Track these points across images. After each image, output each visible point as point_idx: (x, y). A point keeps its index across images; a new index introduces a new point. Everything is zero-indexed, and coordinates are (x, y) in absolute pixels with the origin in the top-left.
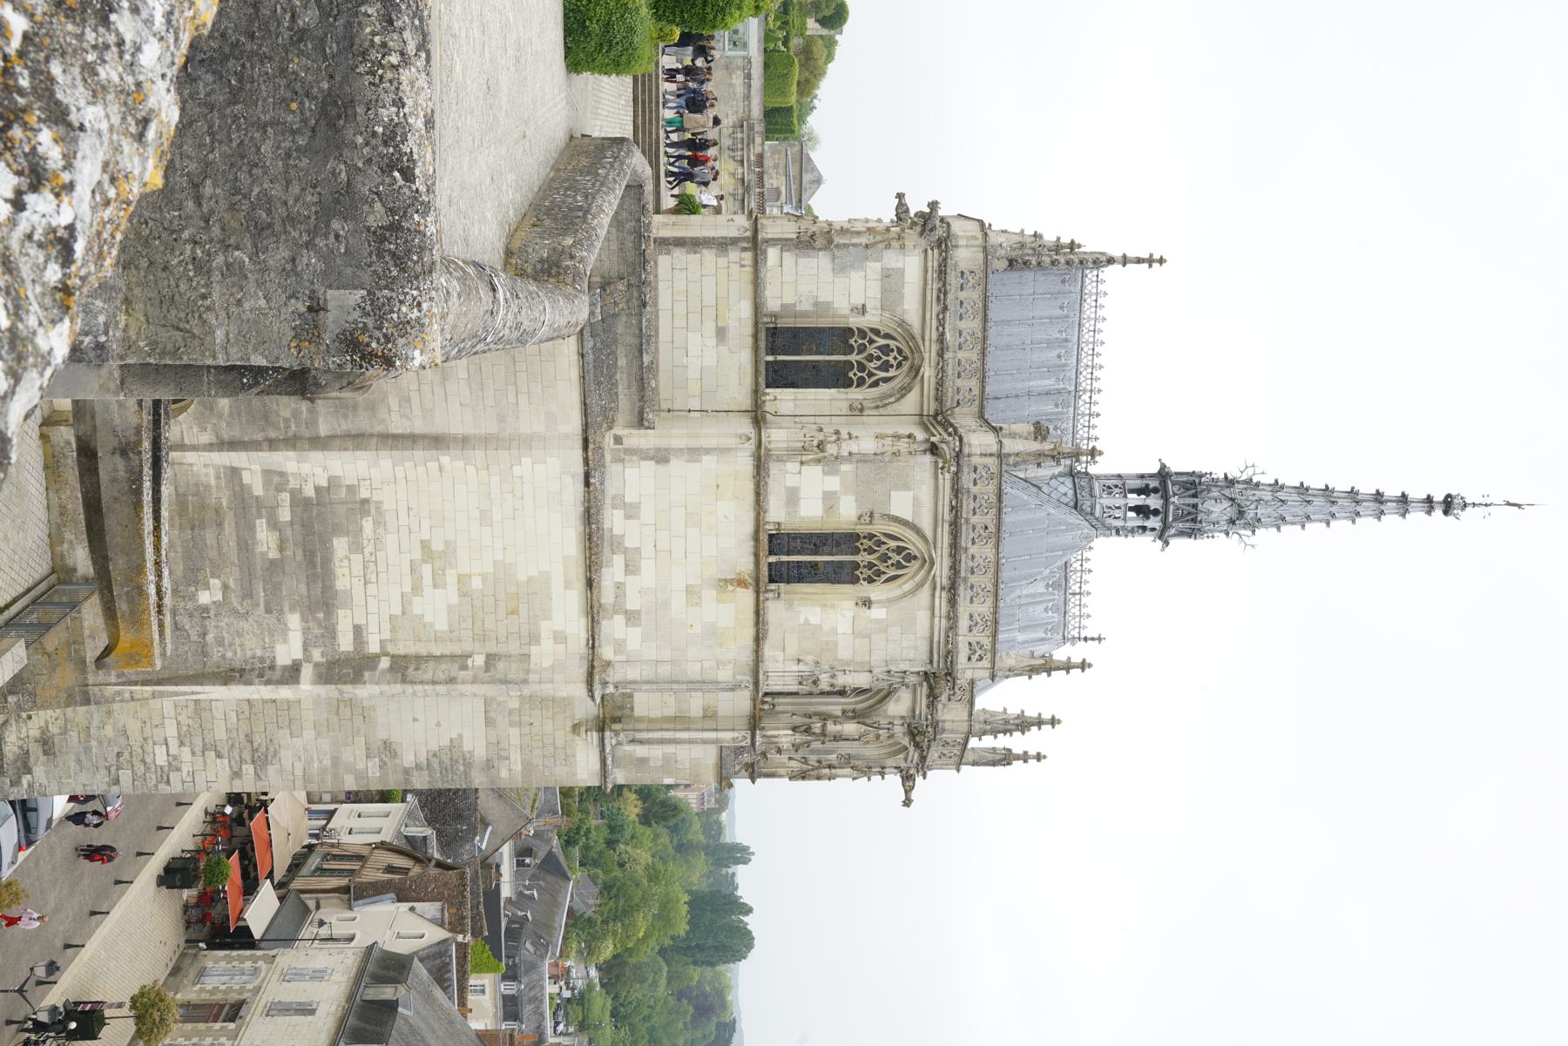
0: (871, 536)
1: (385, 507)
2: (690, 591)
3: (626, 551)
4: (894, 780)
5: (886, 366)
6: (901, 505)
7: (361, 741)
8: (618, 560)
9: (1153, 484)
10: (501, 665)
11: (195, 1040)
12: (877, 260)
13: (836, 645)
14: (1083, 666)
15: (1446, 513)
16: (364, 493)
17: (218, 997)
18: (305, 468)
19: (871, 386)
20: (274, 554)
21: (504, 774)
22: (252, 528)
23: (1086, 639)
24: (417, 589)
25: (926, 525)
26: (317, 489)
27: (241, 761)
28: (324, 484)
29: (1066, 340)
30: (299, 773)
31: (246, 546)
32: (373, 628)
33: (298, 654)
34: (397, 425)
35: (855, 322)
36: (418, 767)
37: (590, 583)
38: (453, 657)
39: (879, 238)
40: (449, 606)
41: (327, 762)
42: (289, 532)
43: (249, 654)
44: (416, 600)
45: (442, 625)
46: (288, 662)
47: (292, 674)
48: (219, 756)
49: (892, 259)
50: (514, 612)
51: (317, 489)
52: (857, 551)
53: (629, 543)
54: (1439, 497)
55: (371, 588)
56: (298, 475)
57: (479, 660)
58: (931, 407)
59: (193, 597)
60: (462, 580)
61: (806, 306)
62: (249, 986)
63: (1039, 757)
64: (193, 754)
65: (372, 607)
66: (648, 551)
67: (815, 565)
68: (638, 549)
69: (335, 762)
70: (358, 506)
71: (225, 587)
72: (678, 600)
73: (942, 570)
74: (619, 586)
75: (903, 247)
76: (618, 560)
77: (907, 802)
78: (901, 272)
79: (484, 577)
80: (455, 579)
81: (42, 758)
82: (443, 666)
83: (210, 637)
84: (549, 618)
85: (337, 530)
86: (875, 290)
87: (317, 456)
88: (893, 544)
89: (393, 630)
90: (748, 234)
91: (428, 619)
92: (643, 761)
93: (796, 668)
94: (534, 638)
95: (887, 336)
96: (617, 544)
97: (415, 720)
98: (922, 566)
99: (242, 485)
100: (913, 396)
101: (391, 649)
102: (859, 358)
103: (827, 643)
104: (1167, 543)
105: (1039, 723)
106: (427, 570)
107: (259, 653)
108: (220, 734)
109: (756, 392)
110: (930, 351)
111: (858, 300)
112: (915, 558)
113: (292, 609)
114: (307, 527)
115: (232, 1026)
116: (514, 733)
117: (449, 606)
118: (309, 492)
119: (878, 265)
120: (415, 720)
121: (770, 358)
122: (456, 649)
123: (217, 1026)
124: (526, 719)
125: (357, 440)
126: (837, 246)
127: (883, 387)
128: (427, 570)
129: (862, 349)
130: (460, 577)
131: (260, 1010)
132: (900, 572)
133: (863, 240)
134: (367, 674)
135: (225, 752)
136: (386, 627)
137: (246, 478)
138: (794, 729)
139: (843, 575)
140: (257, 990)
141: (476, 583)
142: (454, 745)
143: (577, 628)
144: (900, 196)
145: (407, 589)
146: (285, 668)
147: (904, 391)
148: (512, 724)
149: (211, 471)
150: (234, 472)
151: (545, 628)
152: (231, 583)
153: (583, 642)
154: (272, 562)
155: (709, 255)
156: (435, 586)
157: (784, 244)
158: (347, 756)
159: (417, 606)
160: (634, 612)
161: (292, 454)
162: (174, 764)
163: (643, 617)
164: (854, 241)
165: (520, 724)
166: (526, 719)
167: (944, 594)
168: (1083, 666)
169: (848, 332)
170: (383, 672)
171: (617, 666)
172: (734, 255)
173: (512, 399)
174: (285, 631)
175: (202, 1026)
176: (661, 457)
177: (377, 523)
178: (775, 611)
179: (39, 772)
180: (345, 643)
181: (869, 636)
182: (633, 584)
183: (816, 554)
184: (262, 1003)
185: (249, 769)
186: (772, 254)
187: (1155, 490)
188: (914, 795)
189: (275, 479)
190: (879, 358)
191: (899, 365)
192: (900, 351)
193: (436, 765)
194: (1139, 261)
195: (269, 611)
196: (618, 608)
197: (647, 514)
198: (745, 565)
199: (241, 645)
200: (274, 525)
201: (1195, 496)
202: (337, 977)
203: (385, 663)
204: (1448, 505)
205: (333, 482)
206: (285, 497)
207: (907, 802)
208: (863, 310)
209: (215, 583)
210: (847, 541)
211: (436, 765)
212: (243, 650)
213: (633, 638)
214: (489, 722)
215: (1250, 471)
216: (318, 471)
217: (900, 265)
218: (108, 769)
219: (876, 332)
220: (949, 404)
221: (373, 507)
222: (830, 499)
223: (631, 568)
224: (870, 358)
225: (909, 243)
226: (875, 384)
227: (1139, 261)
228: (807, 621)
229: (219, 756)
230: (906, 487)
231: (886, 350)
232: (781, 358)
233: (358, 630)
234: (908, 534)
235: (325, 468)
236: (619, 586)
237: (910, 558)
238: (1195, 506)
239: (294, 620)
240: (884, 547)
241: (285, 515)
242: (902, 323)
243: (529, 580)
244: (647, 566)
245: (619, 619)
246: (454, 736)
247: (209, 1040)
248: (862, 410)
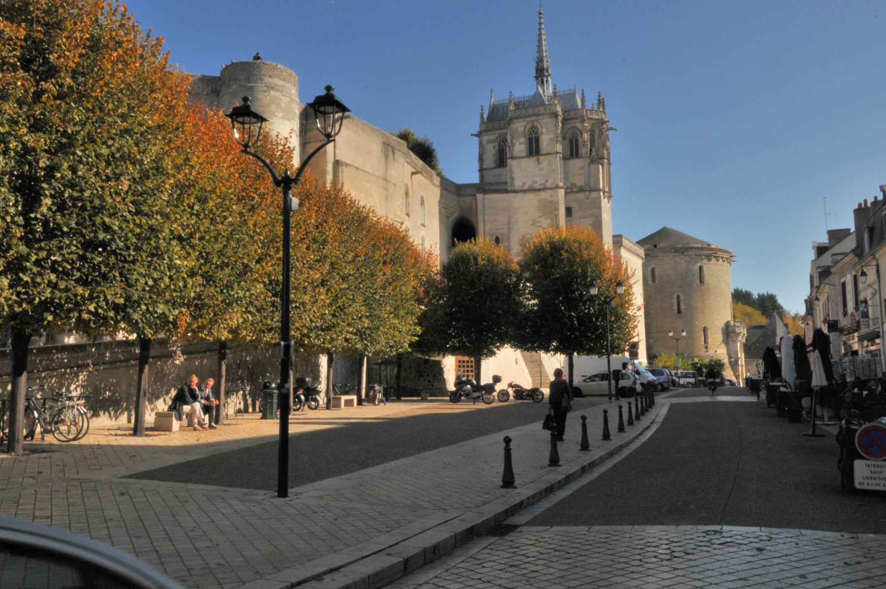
2: (541, 169)
6: (521, 129)
25: (525, 123)
34: (506, 230)
35: (497, 148)
37: (539, 190)
45: (549, 221)
49: (484, 142)
53: (530, 183)
60: (539, 217)
61: (494, 159)
73: (534, 118)
87: (512, 246)
94: (551, 201)
96: (531, 186)
110: (501, 131)
125: (509, 238)
139: (537, 140)
142: (592, 225)
143: (549, 192)
151: (550, 199)
176: (513, 179)
186: (485, 167)
196: (544, 184)
197: (525, 180)
198: (533, 160)
205: (519, 243)
210: (530, 141)
213: (550, 181)
222: (521, 144)
223: (536, 182)
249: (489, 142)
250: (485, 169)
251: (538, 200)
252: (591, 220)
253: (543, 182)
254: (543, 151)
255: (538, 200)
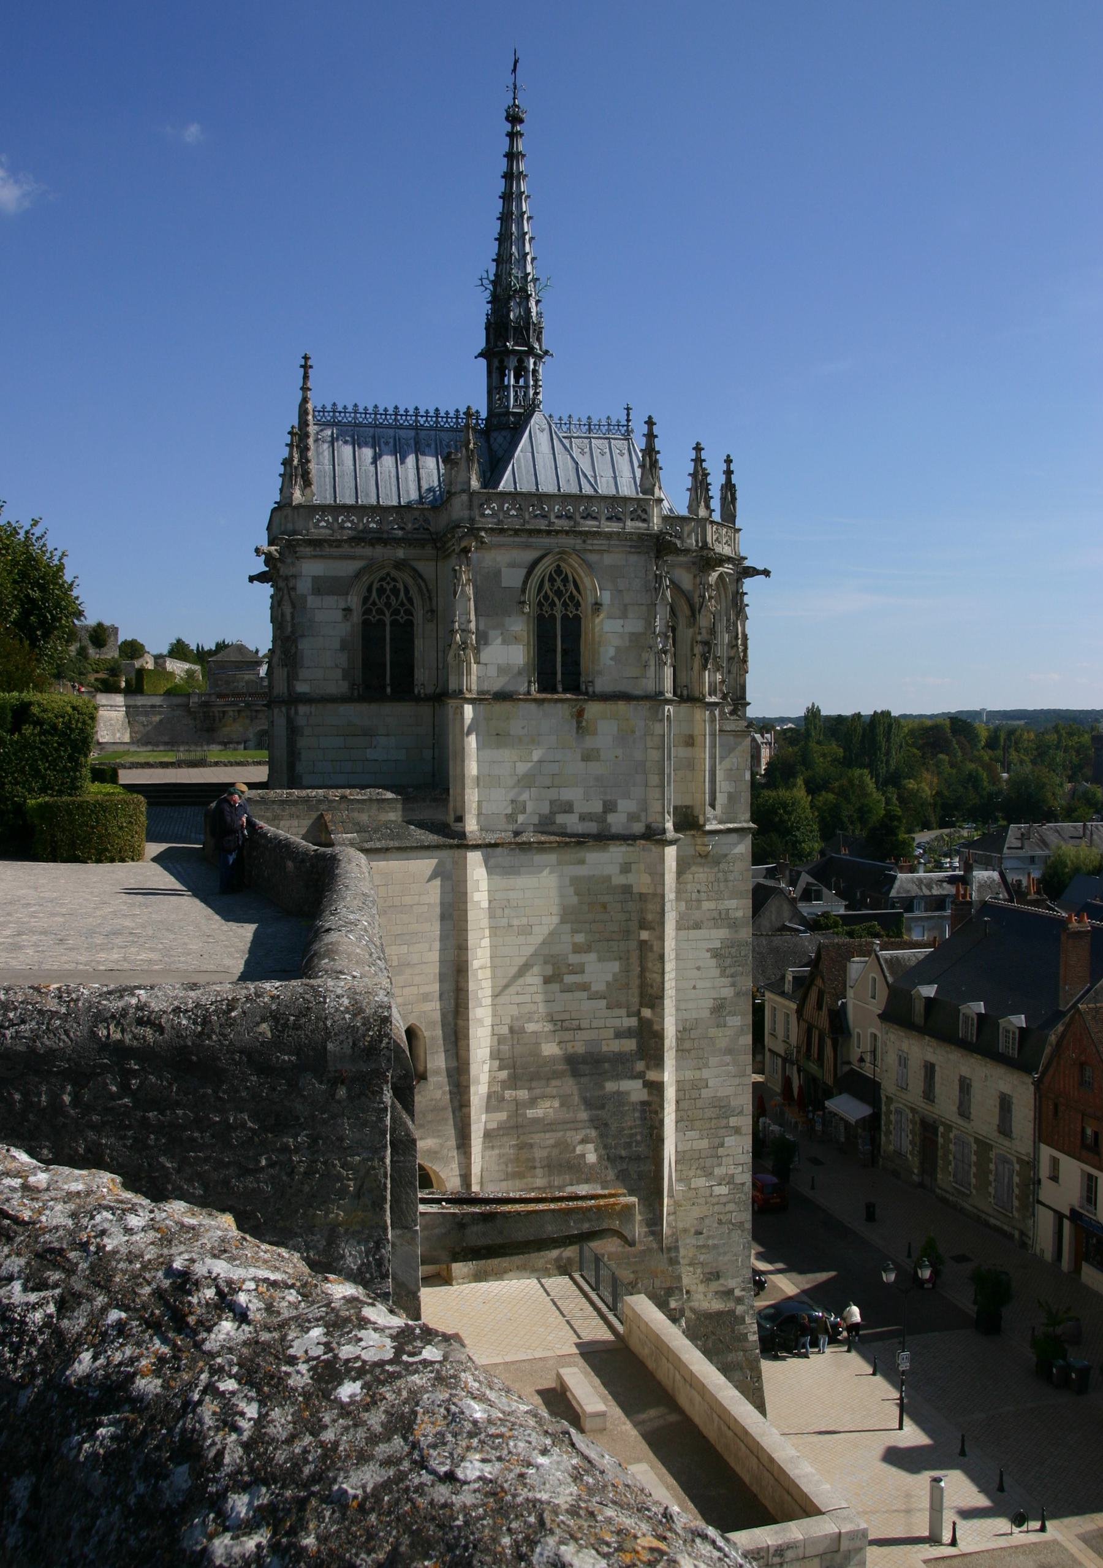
0: (540, 604)
1: (516, 1013)
2: (587, 758)
3: (553, 813)
4: (748, 584)
5: (395, 591)
6: (513, 578)
7: (712, 1032)
8: (560, 819)
9: (496, 363)
10: (650, 917)
11: (951, 1157)
12: (304, 598)
13: (633, 634)
14: (650, 423)
15: (521, 121)
16: (505, 1030)
17: (917, 1139)
18: (484, 1078)
19: (412, 604)
20: (556, 1104)
21: (739, 914)
22: (535, 1121)
23: (628, 420)
24: (585, 987)
25: (530, 556)
26: (501, 1068)
27: (727, 1127)
28: (497, 1063)
29: (374, 437)
30: (737, 1081)
31: (548, 1126)
32: (617, 1023)
33: (637, 1084)
35: (356, 617)
36: (733, 985)
37: (581, 841)
38: (642, 959)
39: (286, 597)
40: (600, 960)
41: (728, 1059)
42: (537, 1092)
43: (638, 1122)
44: (595, 987)
45: (615, 967)
46: (645, 1090)
47: (657, 1088)
48: (722, 1145)
49: (304, 586)
50: (604, 906)
51: (501, 1068)
52: (553, 617)
53: (546, 809)
54: (508, 127)
55: (585, 1024)
56: (490, 1084)
57: (645, 935)
58: (429, 551)
59: (592, 1167)
60: (577, 949)
61: (343, 659)
62: (910, 1116)
63: (728, 461)
64: (720, 1165)
65: (601, 1023)
66: (553, 794)
67: (564, 652)
68: (552, 802)
69: (729, 1051)
70: (515, 1036)
71: (584, 1141)
72: (596, 768)
74: (583, 818)
75: (294, 576)
76: (560, 819)
77: (766, 573)
78: (315, 579)
79: (574, 932)
80: (578, 955)
81: (722, 1281)
82: (650, 965)
83: (623, 1153)
84: (609, 877)
85: (536, 1053)
86: (330, 601)
88: (547, 585)
89: (619, 1006)
90: (284, 709)
91: (610, 978)
92: (732, 798)
93: (653, 668)
94: (627, 889)
95: (369, 590)
97: (694, 988)
98: (564, 560)
99: (498, 1128)
100: (422, 567)
101: (634, 1009)
102: (388, 614)
103: (631, 641)
104: (546, 353)
105: (698, 461)
106: (569, 979)
107: (637, 1115)
108: (704, 1144)
109: (418, 699)
111: (338, 615)
112: (558, 566)
113: (603, 1088)
114: (534, 1077)
115: (941, 1129)
116: (707, 905)
117: (600, 960)
118: (504, 1074)
119: (310, 599)
120: (694, 988)
121: (389, 690)
122: (635, 955)
123: (941, 1140)
124: (694, 896)
126: (292, 632)
127: (414, 592)
128: (569, 979)
129: (380, 612)
130: (574, 952)
131: (930, 1108)
132: (571, 578)
133: (288, 609)
134: (656, 1027)
135: (717, 1141)
136: (617, 1012)
137: (493, 1125)
138: (705, 667)
139: (573, 629)
140: (913, 1110)
141: (580, 938)
142: (716, 954)
143: (617, 853)
144: (252, 579)
145: (585, 995)
146: (650, 1094)
147: (417, 575)
148: (699, 908)
149: (488, 1153)
150: (488, 1135)
151: (619, 880)
152: (579, 1137)
153: (631, 849)
154: (562, 1105)
155: (302, 743)
156: (583, 972)
157: (292, 677)
158: (722, 1043)
159: (599, 986)
160: (604, 805)
161: (472, 1089)
162: (729, 1180)
163: (609, 798)
164: (289, 618)
165: (699, 901)
166: (694, 896)
167: (589, 542)
168: (650, 423)
169: (365, 623)
170: (654, 1013)
171: (650, 820)
172: (301, 721)
173: (425, 908)
174: (619, 1093)
175: (940, 1153)
177: (530, 1020)
178: (602, 685)
179: (731, 1283)
180: (630, 1045)
181: (626, 606)
182: (580, 807)
183: (555, 651)
184: (923, 1105)
185: (733, 1121)
186: (301, 688)
187: (501, 362)
188: (761, 568)
189: (494, 1101)
190: (388, 597)
191: (394, 580)
192: (382, 579)
193: (733, 970)
194: (306, 377)
195: (603, 1107)
196: (601, 819)
199: (631, 1128)
200: (533, 1102)
201: (507, 329)
202: (905, 1046)
203: (647, 1013)
204: (514, 118)
205: (495, 1055)
206: (508, 1094)
207: (766, 573)
208: (347, 610)
209: (579, 1150)
211: (733, 970)
212: (635, 1127)
213: (626, 806)
214: (697, 926)
215: (485, 282)
216: (486, 1067)
217: (310, 580)
218: (730, 1231)
219: (365, 600)
220: (427, 537)
221: (516, 1024)
223: (568, 808)
224: (388, 605)
225: (291, 571)
226: (410, 600)
227: (306, 377)
228: (611, 659)
229: (722, 1145)
230: (498, 574)
231: (381, 591)
232: (388, 681)
233: (619, 1035)
234: (539, 571)
235: (484, 1062)
236: (583, 818)
237: (559, 570)
238: (515, 328)
239: (610, 1086)
240: (549, 592)
241: (523, 1094)
242: (358, 575)
243: (577, 894)
244: (567, 794)
245: (611, 818)
246: (709, 955)
247: (952, 1147)
248: (432, 611)
249: (324, 587)
250: (307, 699)
251: (575, 881)
252: (717, 936)
253: (597, 807)
254: (602, 685)
255: (575, 881)
